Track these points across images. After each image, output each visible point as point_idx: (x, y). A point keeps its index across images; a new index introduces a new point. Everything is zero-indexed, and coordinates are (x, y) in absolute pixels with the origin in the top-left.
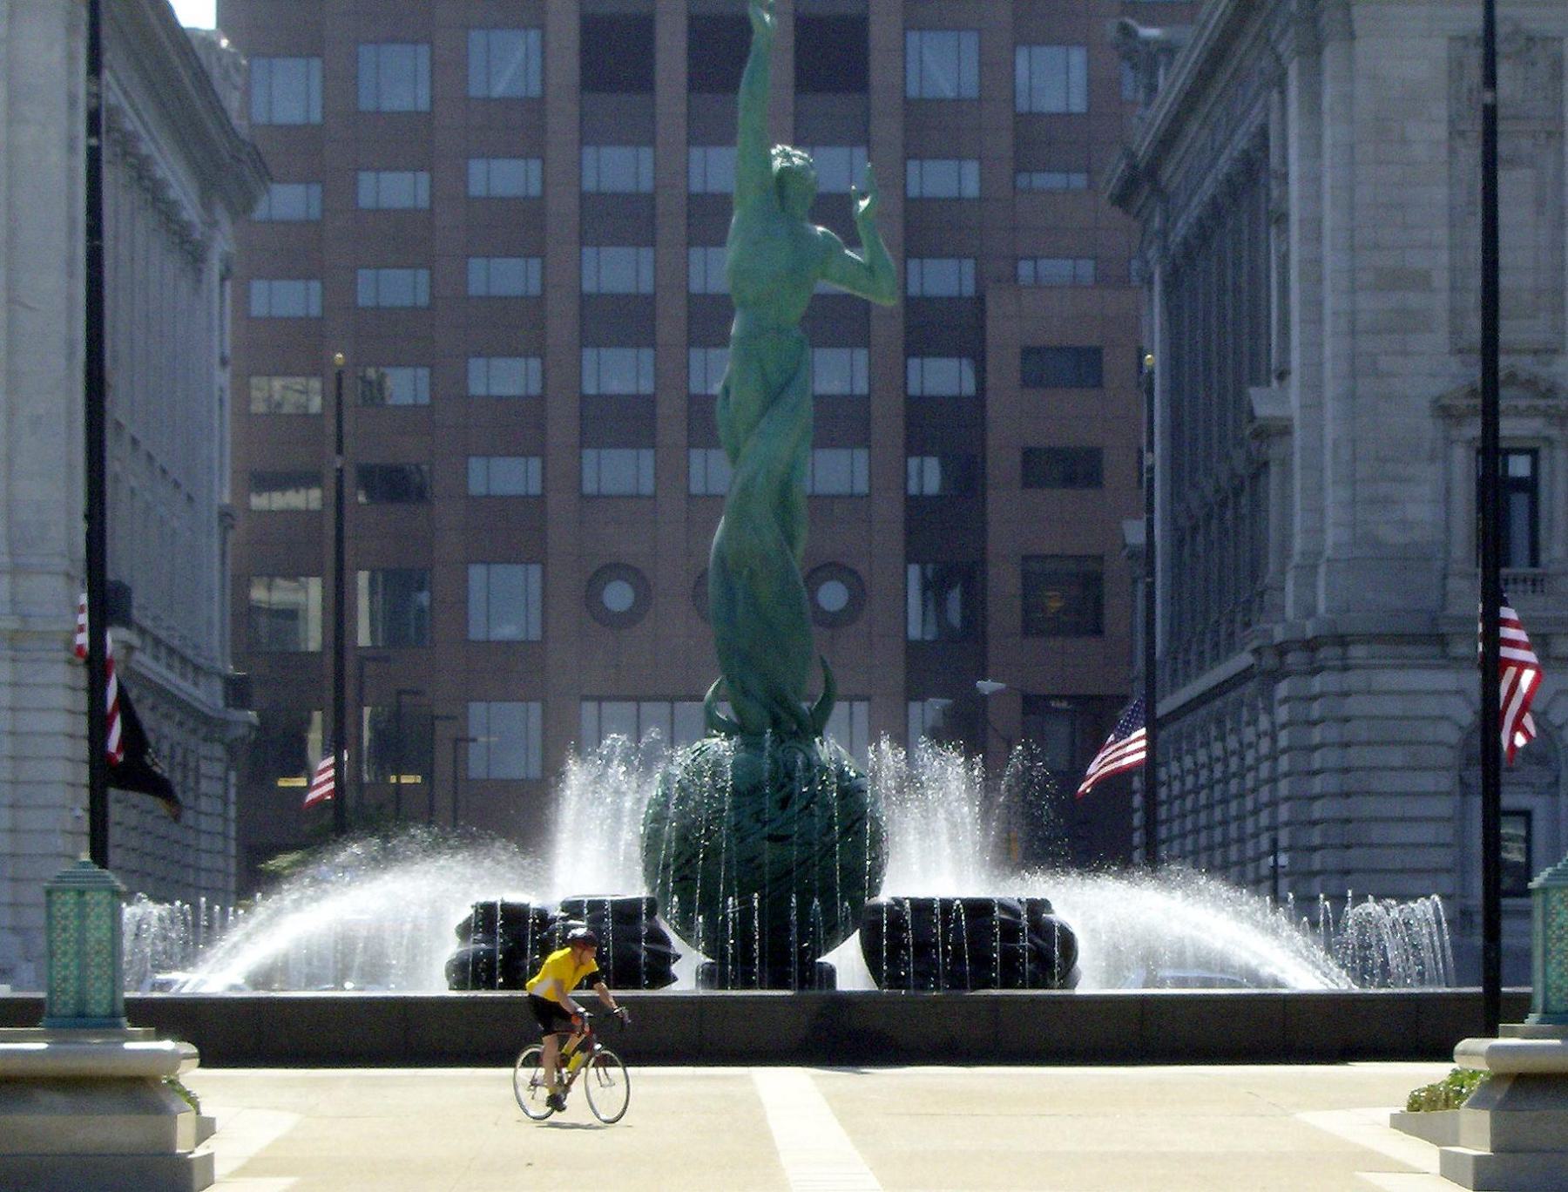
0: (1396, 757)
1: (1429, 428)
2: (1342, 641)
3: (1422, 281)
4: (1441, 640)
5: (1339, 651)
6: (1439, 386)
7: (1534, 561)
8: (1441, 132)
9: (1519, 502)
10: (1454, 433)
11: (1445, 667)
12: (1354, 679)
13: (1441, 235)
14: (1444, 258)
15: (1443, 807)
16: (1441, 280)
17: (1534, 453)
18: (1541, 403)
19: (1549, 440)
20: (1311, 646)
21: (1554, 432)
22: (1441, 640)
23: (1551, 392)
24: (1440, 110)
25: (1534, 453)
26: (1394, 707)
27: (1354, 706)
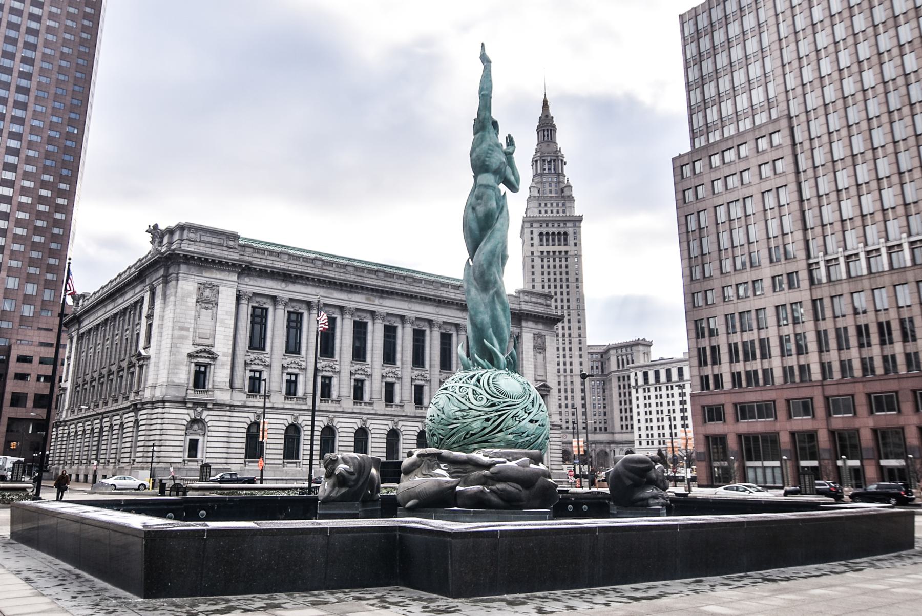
0: (173, 427)
2: (164, 402)
3: (187, 329)
6: (189, 351)
7: (204, 387)
8: (194, 301)
9: (202, 376)
12: (165, 410)
13: (192, 321)
14: (193, 325)
15: (182, 438)
16: (191, 330)
19: (210, 364)
22: (185, 403)
23: (213, 354)
24: (195, 297)
26: (174, 416)
27: (166, 416)
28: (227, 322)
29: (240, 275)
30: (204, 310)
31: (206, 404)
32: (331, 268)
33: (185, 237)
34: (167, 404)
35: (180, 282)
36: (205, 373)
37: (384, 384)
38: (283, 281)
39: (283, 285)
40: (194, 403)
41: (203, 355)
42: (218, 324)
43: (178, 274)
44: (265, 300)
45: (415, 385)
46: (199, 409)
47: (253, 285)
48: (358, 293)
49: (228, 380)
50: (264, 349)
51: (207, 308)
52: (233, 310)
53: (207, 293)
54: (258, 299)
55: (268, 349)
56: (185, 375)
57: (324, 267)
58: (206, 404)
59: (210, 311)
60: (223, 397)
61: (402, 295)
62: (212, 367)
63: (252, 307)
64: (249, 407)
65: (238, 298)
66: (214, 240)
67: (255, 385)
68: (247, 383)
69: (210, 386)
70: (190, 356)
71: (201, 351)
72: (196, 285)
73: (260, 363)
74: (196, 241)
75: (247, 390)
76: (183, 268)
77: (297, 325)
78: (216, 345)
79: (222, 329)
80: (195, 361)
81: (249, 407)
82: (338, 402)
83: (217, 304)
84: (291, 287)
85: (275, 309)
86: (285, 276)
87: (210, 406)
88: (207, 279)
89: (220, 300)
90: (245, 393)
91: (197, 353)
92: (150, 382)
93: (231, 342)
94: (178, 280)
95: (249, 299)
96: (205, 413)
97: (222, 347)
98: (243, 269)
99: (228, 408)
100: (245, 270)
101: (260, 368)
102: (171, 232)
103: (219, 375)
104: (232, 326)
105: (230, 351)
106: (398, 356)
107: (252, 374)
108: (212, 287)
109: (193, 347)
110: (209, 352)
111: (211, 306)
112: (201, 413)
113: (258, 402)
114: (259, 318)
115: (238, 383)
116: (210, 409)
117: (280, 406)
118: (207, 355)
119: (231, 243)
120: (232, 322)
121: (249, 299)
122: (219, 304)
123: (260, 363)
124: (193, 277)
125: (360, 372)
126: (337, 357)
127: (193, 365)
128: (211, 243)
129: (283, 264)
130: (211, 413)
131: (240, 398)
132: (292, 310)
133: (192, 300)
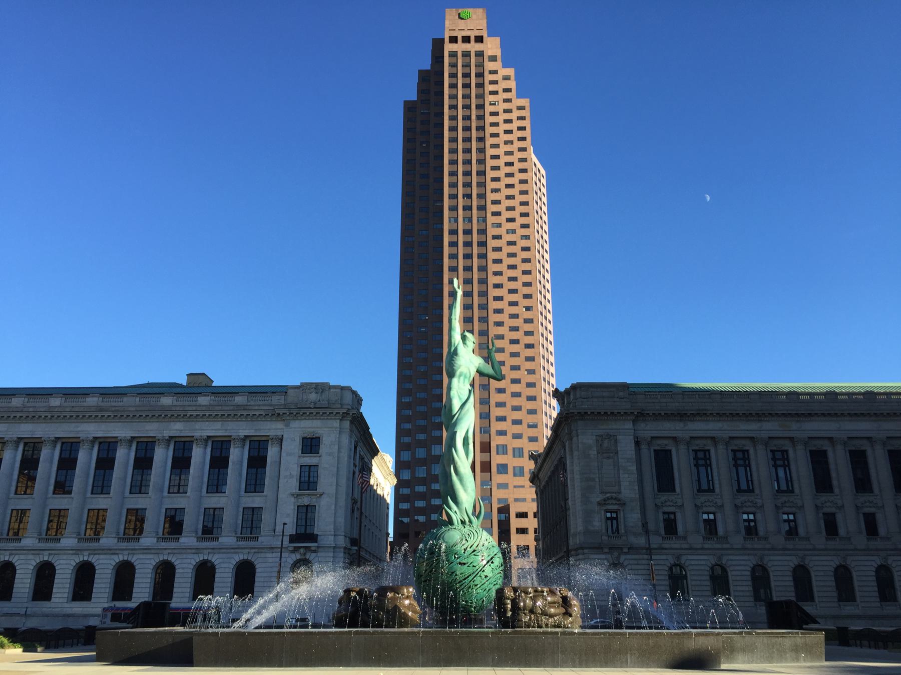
1: (597, 508)
4: (602, 548)
5: (582, 551)
6: (598, 499)
8: (596, 452)
9: (615, 522)
10: (602, 508)
11: (603, 554)
14: (597, 475)
17: (616, 512)
18: (618, 503)
20: (576, 550)
21: (620, 508)
22: (602, 548)
23: (619, 500)
24: (595, 449)
25: (616, 512)
28: (629, 468)
29: (634, 421)
30: (605, 460)
31: (621, 549)
32: (732, 400)
33: (578, 396)
34: (586, 551)
35: (579, 437)
36: (616, 518)
37: (821, 515)
38: (681, 420)
39: (682, 424)
40: (610, 548)
41: (610, 502)
42: (621, 472)
43: (577, 431)
44: (665, 442)
45: (864, 514)
46: (616, 554)
47: (649, 429)
48: (768, 421)
49: (640, 524)
50: (674, 490)
51: (608, 458)
52: (634, 456)
53: (606, 444)
54: (698, 442)
55: (678, 490)
56: (598, 523)
57: (724, 400)
58: (621, 549)
59: (611, 460)
60: (641, 541)
61: (823, 415)
62: (622, 513)
63: (655, 450)
64: (666, 549)
65: (637, 443)
66: (604, 394)
67: (670, 527)
68: (662, 525)
69: (623, 531)
70: (599, 504)
71: (608, 499)
72: (594, 438)
73: (671, 504)
74: (589, 398)
75: (663, 532)
76: (580, 423)
77: (784, 463)
78: (623, 491)
79: (626, 476)
80: (605, 508)
81: (666, 549)
82: (766, 538)
83: (617, 453)
84: (692, 426)
85: (755, 450)
86: (681, 416)
87: (626, 550)
88: (604, 431)
89: (619, 449)
90: (660, 535)
91: (605, 500)
92: (572, 531)
93: (636, 488)
94: (578, 436)
95: (649, 444)
96: (623, 558)
97: (629, 491)
98: (637, 416)
99: (644, 551)
100: (640, 416)
101: (672, 509)
102: (567, 392)
103: (632, 517)
104: (635, 472)
105: (638, 496)
106: (835, 483)
107: (666, 516)
108: (609, 437)
109: (601, 495)
110: (615, 499)
111: (612, 455)
112: (618, 558)
113: (674, 543)
114: (663, 460)
115: (651, 527)
116: (626, 553)
117: (699, 546)
118: (614, 502)
119: (621, 394)
120: (634, 468)
121: (649, 444)
122: (619, 452)
123: (671, 504)
124: (590, 431)
125: (787, 505)
126: (757, 491)
127: (603, 512)
128: (603, 397)
129: (677, 404)
130: (629, 557)
131: (656, 541)
132: (697, 448)
133: (593, 452)
